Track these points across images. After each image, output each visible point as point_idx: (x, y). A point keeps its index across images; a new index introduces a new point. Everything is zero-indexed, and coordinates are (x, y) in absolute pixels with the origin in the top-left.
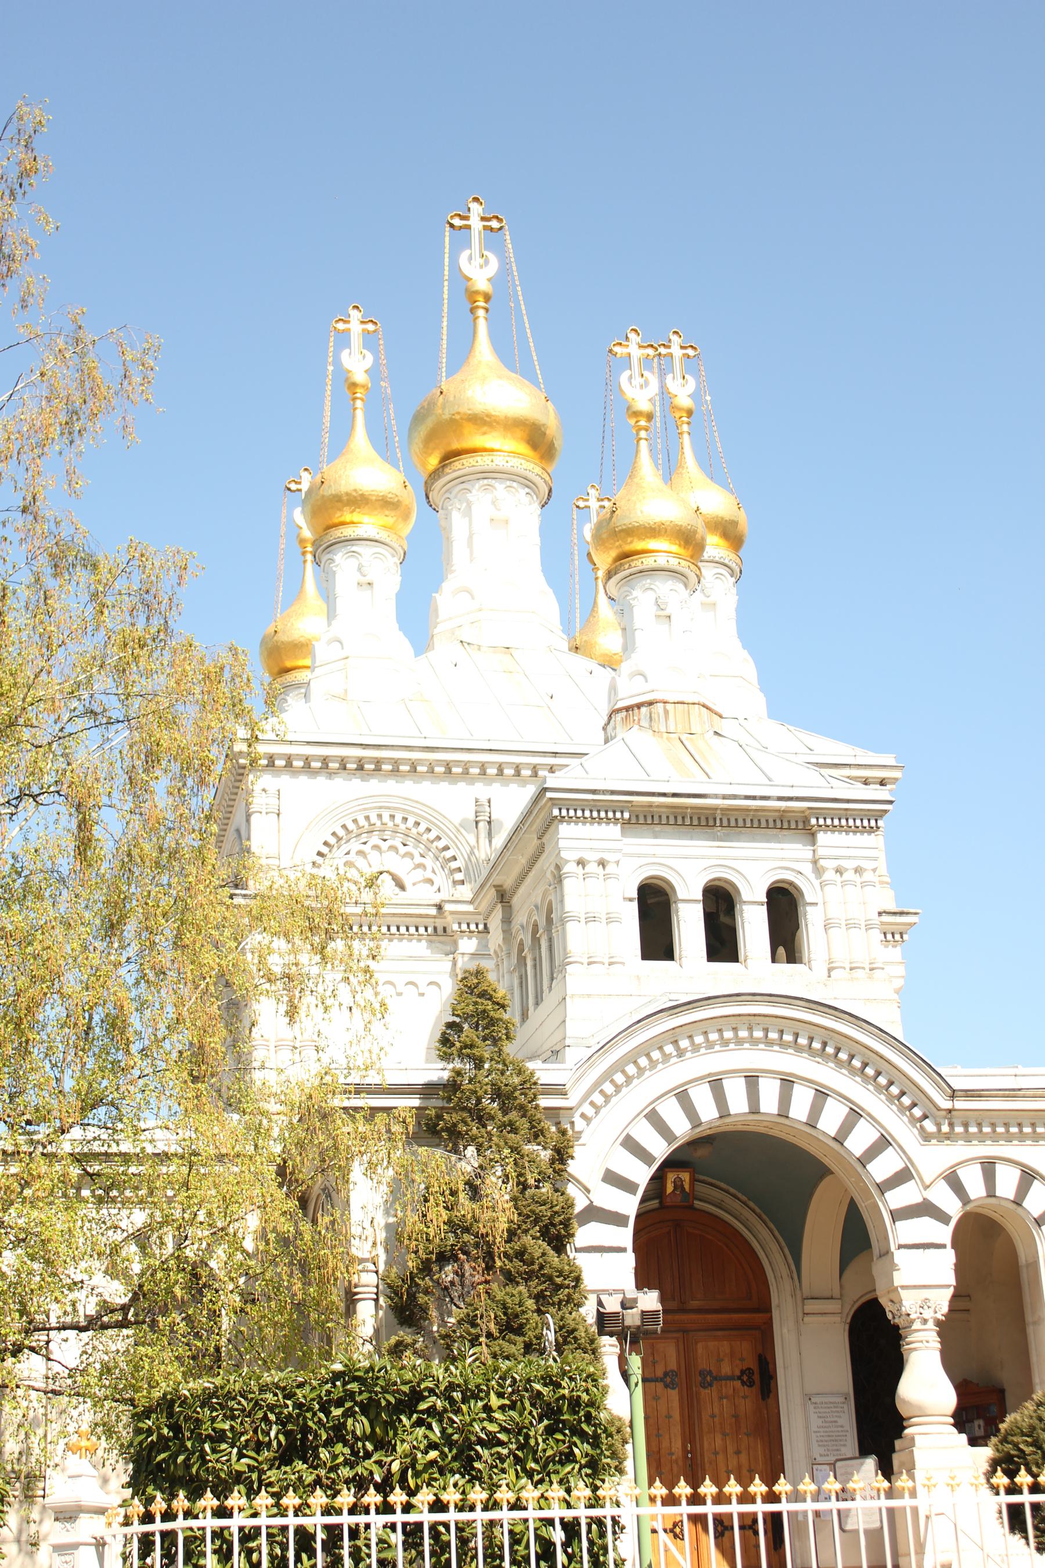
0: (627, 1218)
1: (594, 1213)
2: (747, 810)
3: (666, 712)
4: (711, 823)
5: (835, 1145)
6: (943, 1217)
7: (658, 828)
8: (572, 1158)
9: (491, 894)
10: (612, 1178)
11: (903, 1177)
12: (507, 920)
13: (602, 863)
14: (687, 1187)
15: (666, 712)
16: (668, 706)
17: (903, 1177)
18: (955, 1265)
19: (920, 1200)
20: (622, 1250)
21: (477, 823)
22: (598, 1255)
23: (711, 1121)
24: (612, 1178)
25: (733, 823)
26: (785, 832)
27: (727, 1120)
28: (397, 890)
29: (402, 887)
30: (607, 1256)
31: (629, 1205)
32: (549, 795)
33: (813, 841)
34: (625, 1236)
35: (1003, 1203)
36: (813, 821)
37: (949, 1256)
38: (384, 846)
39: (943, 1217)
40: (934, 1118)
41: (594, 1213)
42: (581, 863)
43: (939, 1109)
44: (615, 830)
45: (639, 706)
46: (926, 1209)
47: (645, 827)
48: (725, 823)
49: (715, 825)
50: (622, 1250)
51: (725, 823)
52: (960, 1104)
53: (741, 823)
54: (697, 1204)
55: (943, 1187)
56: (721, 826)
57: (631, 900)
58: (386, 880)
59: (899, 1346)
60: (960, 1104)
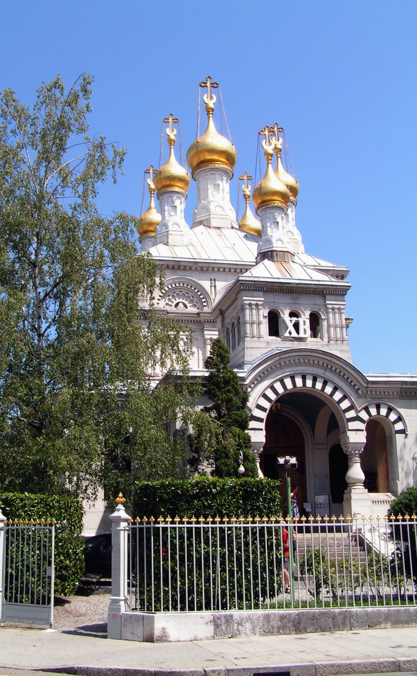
0: (263, 419)
2: (304, 288)
3: (277, 254)
4: (292, 292)
5: (329, 397)
6: (362, 421)
7: (275, 293)
8: (248, 401)
9: (218, 312)
10: (259, 407)
12: (223, 321)
14: (279, 408)
15: (277, 254)
16: (278, 253)
18: (366, 436)
20: (262, 430)
21: (211, 286)
24: (259, 407)
25: (299, 292)
26: (316, 296)
27: (296, 389)
28: (185, 308)
29: (187, 307)
30: (257, 431)
31: (263, 415)
32: (240, 282)
33: (325, 299)
34: (262, 425)
35: (382, 417)
36: (325, 292)
37: (364, 433)
38: (181, 294)
39: (362, 421)
40: (362, 389)
43: (363, 387)
45: (268, 252)
46: (358, 418)
47: (271, 293)
48: (297, 292)
49: (293, 293)
50: (262, 430)
51: (297, 292)
52: (370, 386)
53: (302, 292)
54: (282, 413)
56: (295, 293)
57: (266, 317)
58: (181, 305)
59: (347, 461)
60: (370, 386)
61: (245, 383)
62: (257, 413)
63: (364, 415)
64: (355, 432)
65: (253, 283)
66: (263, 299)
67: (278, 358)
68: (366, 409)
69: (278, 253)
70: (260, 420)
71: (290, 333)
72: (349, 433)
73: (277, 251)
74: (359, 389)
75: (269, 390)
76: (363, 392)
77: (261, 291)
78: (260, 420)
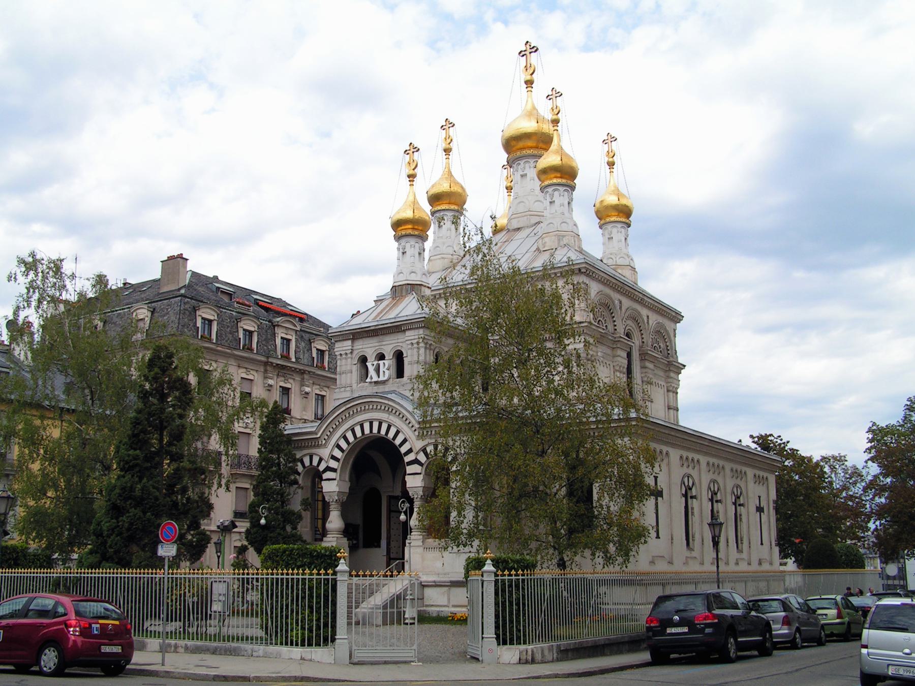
1: (328, 469)
6: (421, 464)
10: (334, 458)
11: (410, 451)
13: (346, 354)
17: (410, 451)
19: (414, 458)
20: (335, 479)
22: (328, 481)
23: (360, 437)
24: (334, 458)
30: (331, 481)
32: (329, 335)
39: (421, 464)
41: (328, 469)
42: (341, 355)
44: (349, 343)
46: (416, 461)
50: (335, 479)
55: (422, 453)
61: (318, 436)
62: (333, 464)
63: (422, 458)
64: (412, 476)
65: (339, 333)
66: (350, 347)
67: (344, 408)
68: (424, 450)
69: (397, 288)
70: (334, 470)
71: (371, 378)
72: (407, 478)
73: (395, 286)
74: (415, 430)
75: (342, 439)
76: (419, 432)
77: (348, 339)
78: (334, 470)
